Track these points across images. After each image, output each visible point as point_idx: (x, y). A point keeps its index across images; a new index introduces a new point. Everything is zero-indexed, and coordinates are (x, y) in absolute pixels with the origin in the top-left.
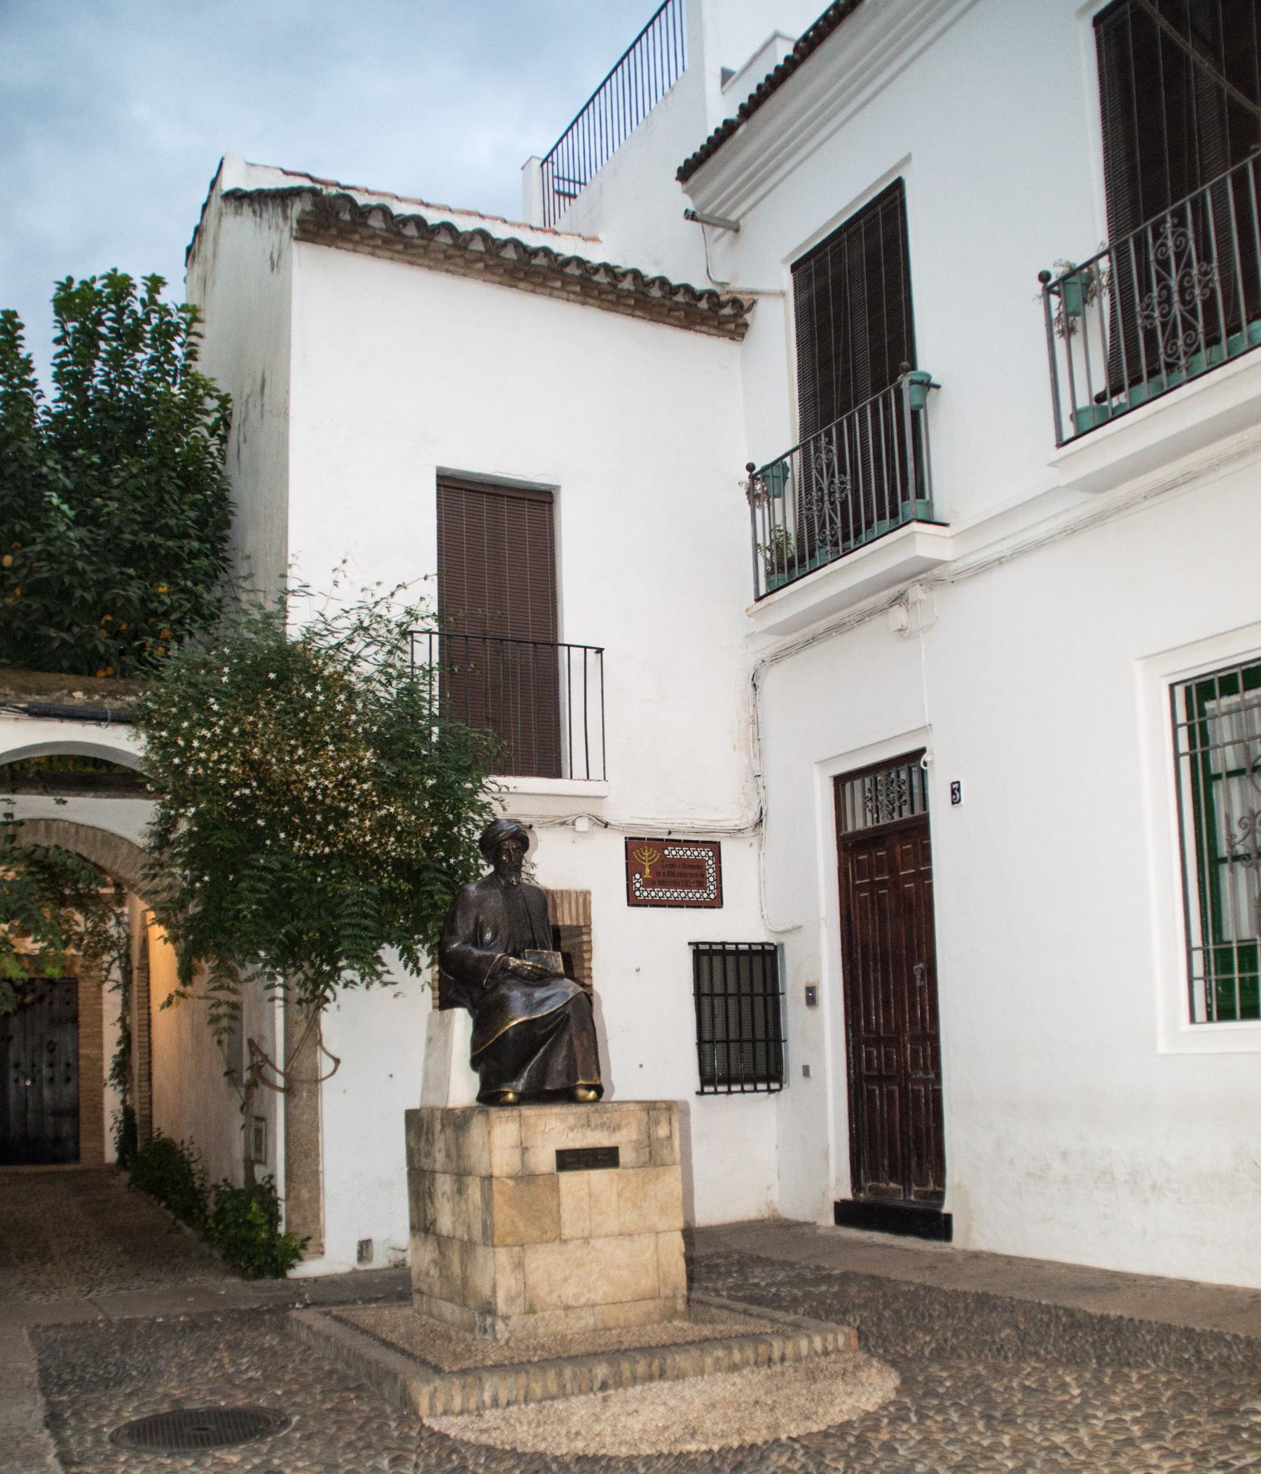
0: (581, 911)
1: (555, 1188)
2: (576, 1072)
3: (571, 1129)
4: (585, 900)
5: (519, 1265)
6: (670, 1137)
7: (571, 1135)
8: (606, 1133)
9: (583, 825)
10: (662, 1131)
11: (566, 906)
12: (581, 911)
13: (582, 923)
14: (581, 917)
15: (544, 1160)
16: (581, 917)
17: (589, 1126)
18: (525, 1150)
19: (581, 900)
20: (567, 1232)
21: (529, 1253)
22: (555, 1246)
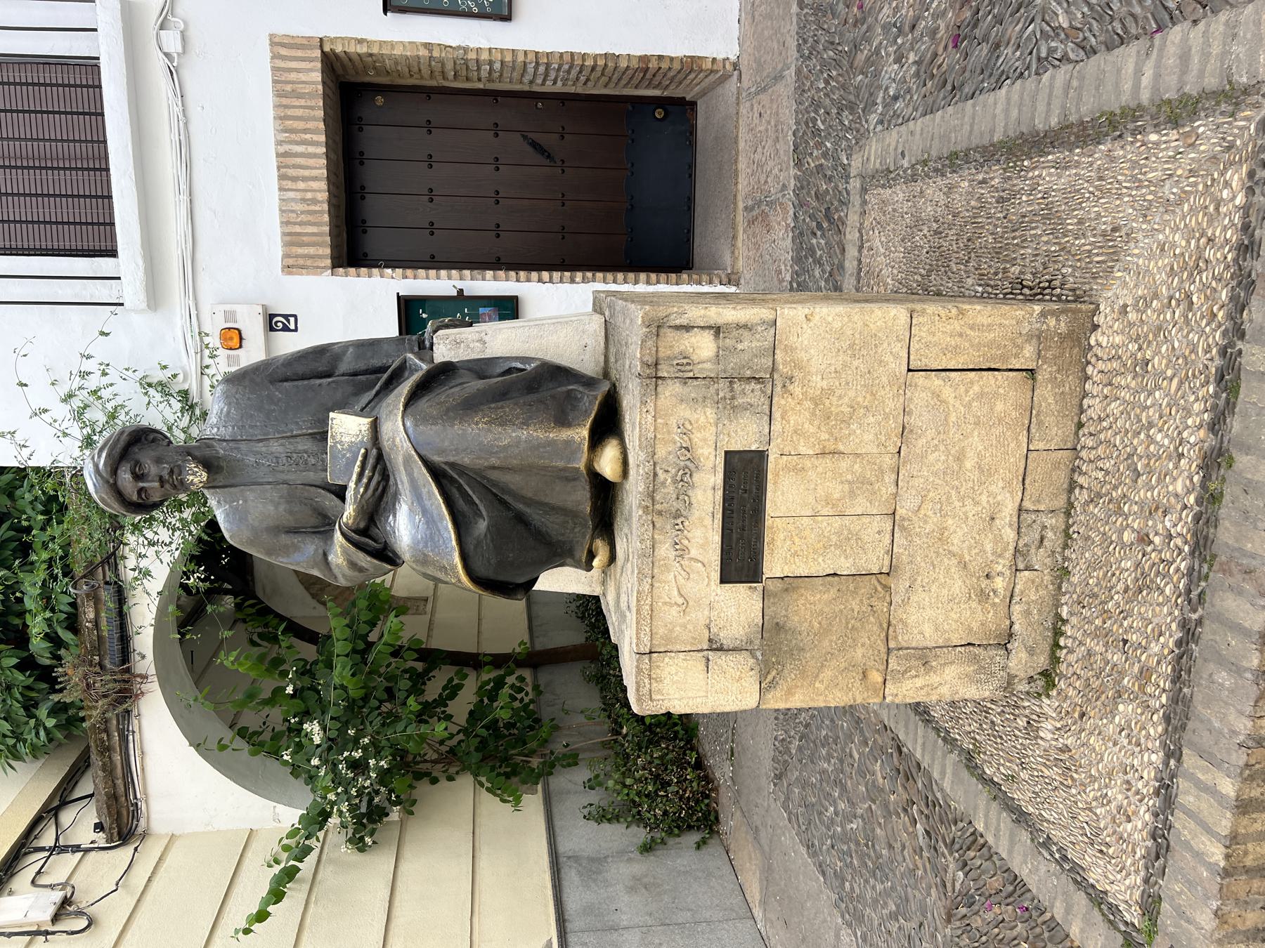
0: (299, 53)
1: (791, 583)
2: (565, 469)
3: (681, 551)
4: (283, 45)
5: (924, 657)
6: (717, 330)
7: (694, 553)
8: (696, 477)
9: (171, 41)
10: (703, 347)
11: (293, 76)
12: (299, 53)
13: (318, 53)
14: (309, 53)
15: (738, 608)
16: (309, 53)
17: (678, 515)
18: (716, 646)
19: (284, 52)
20: (874, 561)
21: (903, 640)
22: (899, 586)
